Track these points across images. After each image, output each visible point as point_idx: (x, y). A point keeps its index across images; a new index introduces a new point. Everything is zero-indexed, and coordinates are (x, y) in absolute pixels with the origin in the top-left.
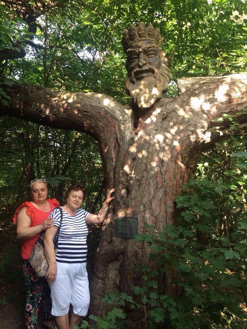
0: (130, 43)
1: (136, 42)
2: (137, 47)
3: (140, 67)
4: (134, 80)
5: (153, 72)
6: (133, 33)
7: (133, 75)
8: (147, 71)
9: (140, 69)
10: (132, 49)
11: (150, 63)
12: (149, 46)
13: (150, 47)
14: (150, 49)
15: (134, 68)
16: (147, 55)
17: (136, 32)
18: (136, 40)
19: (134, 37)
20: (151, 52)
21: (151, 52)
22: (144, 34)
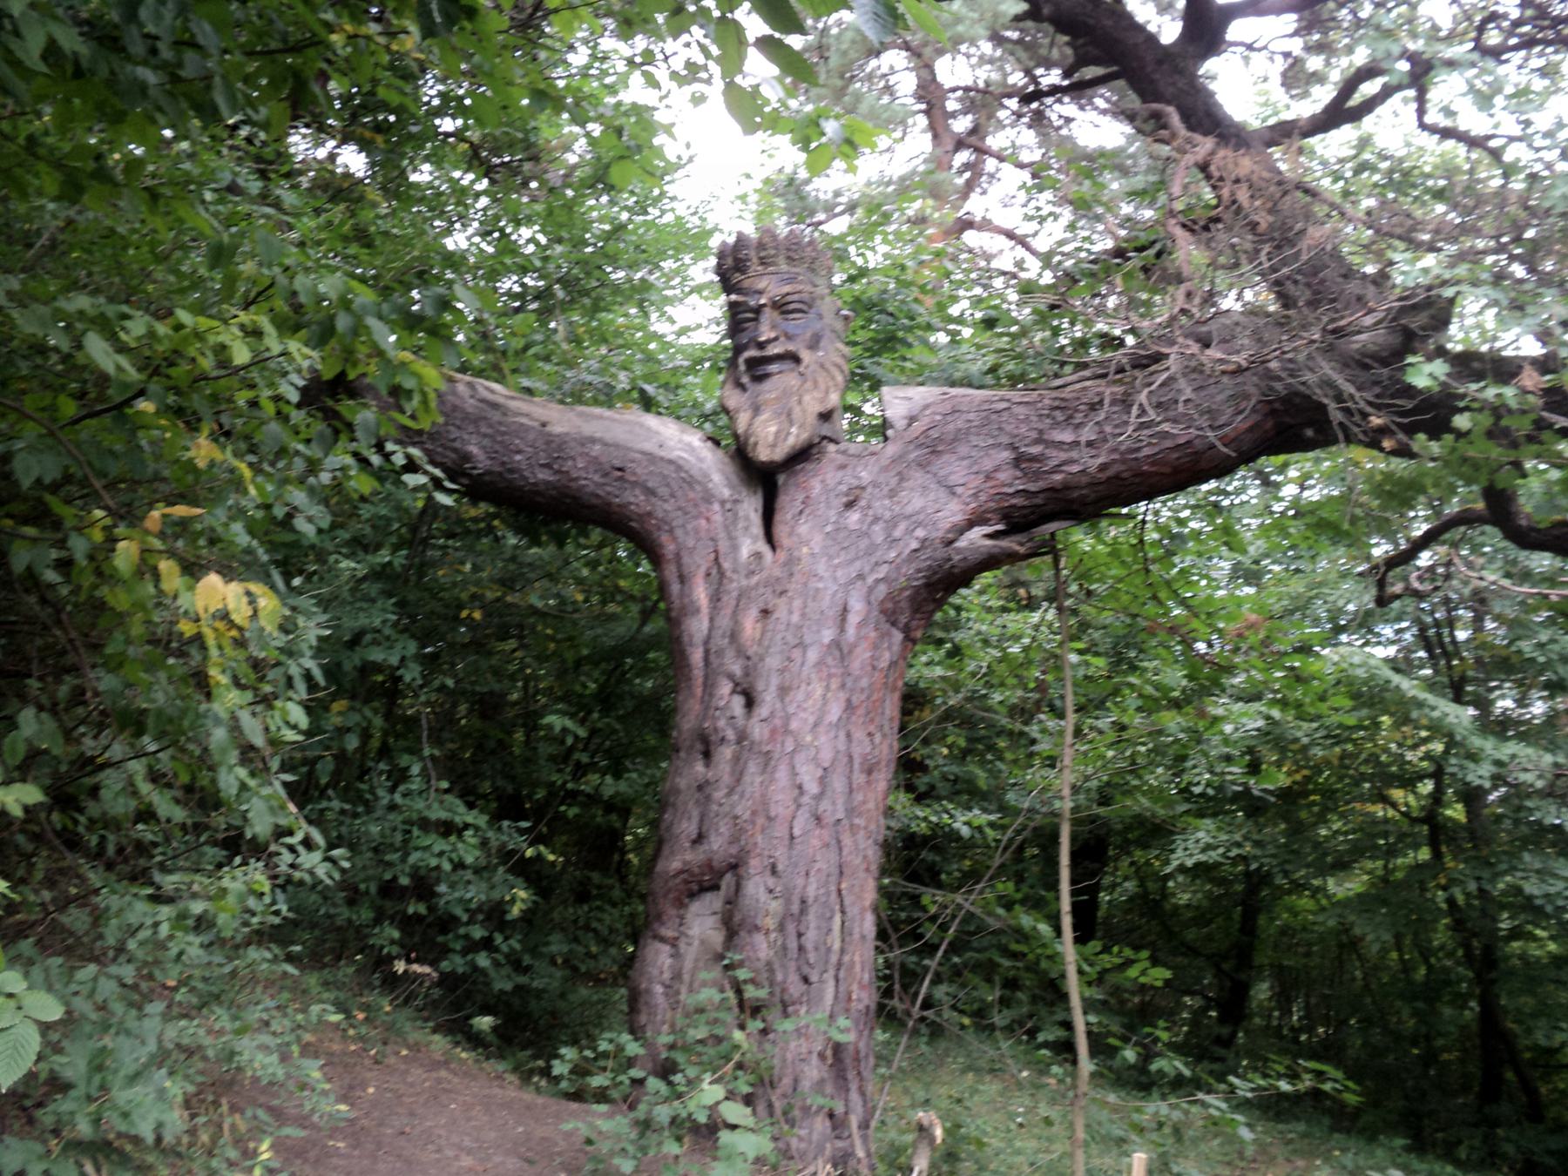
3: (761, 346)
4: (745, 380)
5: (796, 359)
7: (742, 367)
11: (789, 337)
12: (787, 289)
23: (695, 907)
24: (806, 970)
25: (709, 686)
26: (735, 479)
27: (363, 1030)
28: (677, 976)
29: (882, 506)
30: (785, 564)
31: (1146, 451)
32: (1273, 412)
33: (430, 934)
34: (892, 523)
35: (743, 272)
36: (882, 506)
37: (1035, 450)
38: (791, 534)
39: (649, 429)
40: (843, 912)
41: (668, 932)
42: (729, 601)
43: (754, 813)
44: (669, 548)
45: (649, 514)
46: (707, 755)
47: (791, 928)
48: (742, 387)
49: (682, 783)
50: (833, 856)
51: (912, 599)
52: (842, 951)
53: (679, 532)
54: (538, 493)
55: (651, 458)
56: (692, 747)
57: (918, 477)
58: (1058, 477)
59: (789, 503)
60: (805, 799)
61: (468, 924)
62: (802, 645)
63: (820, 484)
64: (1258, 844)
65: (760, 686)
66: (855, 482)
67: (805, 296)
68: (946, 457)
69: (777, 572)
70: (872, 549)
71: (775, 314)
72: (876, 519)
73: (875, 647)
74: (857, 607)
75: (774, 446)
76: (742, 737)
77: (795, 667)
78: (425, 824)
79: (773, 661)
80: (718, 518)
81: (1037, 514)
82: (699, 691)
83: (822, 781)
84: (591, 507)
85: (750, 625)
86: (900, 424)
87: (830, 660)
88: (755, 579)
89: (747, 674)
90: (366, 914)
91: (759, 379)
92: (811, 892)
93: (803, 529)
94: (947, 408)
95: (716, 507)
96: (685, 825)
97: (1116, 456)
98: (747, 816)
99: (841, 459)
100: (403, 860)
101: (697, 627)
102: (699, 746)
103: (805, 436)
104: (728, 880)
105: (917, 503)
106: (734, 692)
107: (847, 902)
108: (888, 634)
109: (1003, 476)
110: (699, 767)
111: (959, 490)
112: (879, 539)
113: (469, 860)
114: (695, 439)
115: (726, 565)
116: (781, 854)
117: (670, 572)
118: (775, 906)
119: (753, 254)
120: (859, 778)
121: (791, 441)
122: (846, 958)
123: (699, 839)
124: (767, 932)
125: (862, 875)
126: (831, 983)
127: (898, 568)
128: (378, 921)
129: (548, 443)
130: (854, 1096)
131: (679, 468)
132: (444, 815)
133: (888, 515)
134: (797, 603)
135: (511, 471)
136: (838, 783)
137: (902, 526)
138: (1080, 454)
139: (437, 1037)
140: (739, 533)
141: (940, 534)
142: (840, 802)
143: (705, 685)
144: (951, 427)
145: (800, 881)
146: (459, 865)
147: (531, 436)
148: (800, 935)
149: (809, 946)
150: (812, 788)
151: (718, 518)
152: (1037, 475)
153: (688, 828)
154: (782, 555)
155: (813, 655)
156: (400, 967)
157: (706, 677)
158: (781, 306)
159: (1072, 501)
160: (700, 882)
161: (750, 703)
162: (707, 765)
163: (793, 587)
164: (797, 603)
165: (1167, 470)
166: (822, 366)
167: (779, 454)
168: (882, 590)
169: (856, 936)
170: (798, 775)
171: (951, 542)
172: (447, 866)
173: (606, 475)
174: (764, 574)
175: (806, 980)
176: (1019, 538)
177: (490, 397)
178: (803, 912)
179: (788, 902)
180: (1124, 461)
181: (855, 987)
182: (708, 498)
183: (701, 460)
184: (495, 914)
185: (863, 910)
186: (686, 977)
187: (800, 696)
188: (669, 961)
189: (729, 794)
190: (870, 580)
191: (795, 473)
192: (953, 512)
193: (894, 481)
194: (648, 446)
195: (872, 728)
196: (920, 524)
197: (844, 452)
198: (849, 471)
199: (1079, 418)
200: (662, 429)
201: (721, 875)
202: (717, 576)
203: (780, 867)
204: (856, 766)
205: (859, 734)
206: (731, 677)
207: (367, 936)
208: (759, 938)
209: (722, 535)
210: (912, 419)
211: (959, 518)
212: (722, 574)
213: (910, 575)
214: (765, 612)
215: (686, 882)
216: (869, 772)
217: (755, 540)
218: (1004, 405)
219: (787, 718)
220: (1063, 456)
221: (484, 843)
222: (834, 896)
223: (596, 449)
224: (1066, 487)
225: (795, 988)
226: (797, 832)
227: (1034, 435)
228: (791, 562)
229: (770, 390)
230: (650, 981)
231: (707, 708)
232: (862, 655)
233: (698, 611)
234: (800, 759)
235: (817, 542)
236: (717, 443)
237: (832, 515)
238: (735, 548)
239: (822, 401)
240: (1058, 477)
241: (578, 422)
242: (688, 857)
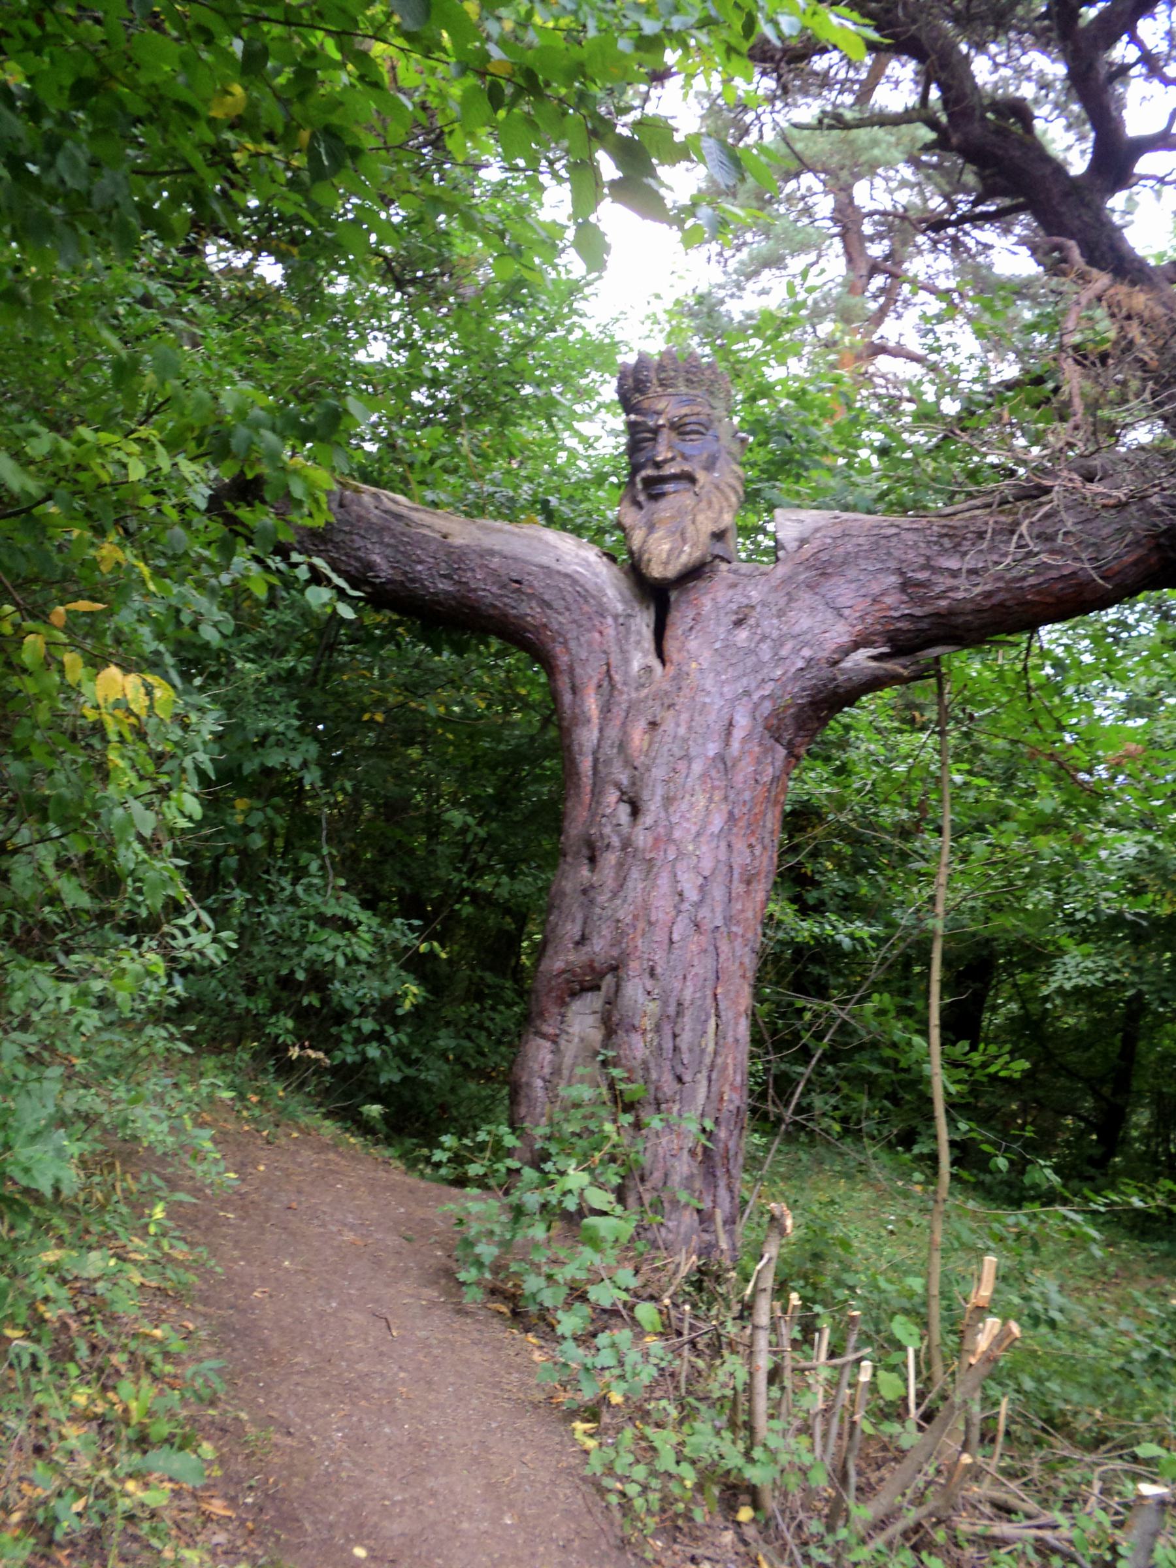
3: (658, 465)
4: (642, 498)
5: (690, 478)
7: (639, 486)
10: (639, 419)
11: (685, 458)
17: (653, 375)
23: (577, 1005)
24: (680, 1070)
25: (597, 793)
26: (628, 594)
27: (257, 1112)
28: (557, 1071)
29: (770, 625)
30: (674, 679)
31: (1032, 581)
32: (1159, 547)
33: (323, 1023)
34: (780, 642)
35: (642, 393)
36: (770, 625)
37: (922, 576)
38: (680, 650)
39: (547, 543)
40: (718, 1016)
41: (549, 1030)
42: (618, 712)
43: (636, 917)
44: (563, 660)
46: (592, 860)
47: (667, 1030)
48: (639, 505)
49: (568, 886)
50: (710, 962)
51: (796, 717)
52: (716, 1053)
53: (572, 644)
54: (439, 603)
55: (547, 570)
56: (578, 853)
57: (806, 598)
59: (680, 619)
60: (685, 906)
61: (360, 1016)
62: (687, 757)
63: (712, 600)
64: (1136, 970)
65: (646, 795)
66: (745, 601)
67: (703, 418)
68: (834, 580)
69: (666, 686)
70: (760, 665)
71: (673, 435)
72: (764, 638)
73: (759, 762)
74: (742, 721)
75: (666, 564)
76: (626, 844)
77: (679, 779)
78: (323, 921)
79: (659, 773)
80: (611, 632)
81: (922, 639)
82: (587, 798)
83: (702, 888)
84: (491, 617)
85: (638, 736)
86: (792, 546)
87: (713, 773)
89: (634, 784)
90: (260, 1004)
91: (655, 497)
92: (688, 995)
93: (693, 644)
94: (837, 532)
95: (610, 620)
96: (569, 926)
97: (1001, 584)
98: (628, 920)
100: (299, 954)
101: (587, 736)
102: (585, 852)
103: (697, 554)
104: (608, 981)
105: (805, 623)
106: (620, 800)
107: (722, 1006)
108: (772, 749)
109: (889, 600)
110: (585, 872)
111: (847, 612)
112: (766, 656)
113: (363, 955)
114: (591, 554)
115: (617, 678)
116: (659, 957)
117: (564, 682)
118: (653, 1007)
119: (653, 375)
120: (738, 887)
121: (684, 559)
122: (719, 1060)
123: (583, 940)
124: (644, 1032)
125: (738, 981)
126: (705, 1083)
127: (784, 686)
128: (274, 1011)
129: (449, 554)
130: (723, 1193)
131: (575, 582)
132: (339, 912)
133: (775, 634)
134: (684, 716)
135: (413, 581)
136: (718, 892)
137: (789, 645)
138: (964, 581)
139: (328, 1123)
140: (631, 647)
141: (826, 654)
142: (719, 910)
143: (593, 793)
144: (841, 550)
145: (677, 985)
146: (353, 960)
147: (433, 547)
148: (675, 1036)
149: (684, 1047)
150: (693, 895)
151: (611, 632)
152: (923, 601)
153: (572, 929)
154: (671, 670)
155: (697, 767)
156: (295, 1053)
157: (594, 784)
158: (679, 428)
159: (956, 627)
160: (581, 982)
161: (636, 811)
162: (592, 870)
164: (684, 716)
165: (1049, 600)
166: (717, 487)
167: (671, 572)
168: (767, 707)
169: (730, 1040)
170: (680, 884)
171: (836, 663)
172: (341, 962)
174: (654, 688)
175: (680, 1079)
176: (902, 660)
177: (394, 507)
178: (679, 1014)
179: (665, 1003)
180: (1008, 590)
181: (726, 1088)
183: (597, 575)
184: (386, 1009)
185: (737, 1016)
186: (566, 1073)
187: (684, 806)
188: (549, 1057)
189: (611, 899)
190: (756, 697)
191: (687, 590)
192: (840, 633)
193: (783, 602)
194: (545, 560)
195: (753, 840)
197: (735, 572)
198: (739, 589)
200: (559, 543)
201: (602, 975)
202: (609, 686)
203: (659, 970)
204: (736, 876)
205: (740, 845)
206: (618, 786)
207: (264, 1026)
208: (636, 1038)
209: (614, 648)
210: (803, 541)
211: (845, 639)
212: (613, 686)
213: (795, 693)
214: (653, 725)
215: (568, 981)
216: (748, 883)
217: (645, 656)
218: (894, 531)
219: (671, 827)
220: (950, 582)
221: (377, 940)
222: (709, 1000)
223: (495, 562)
224: (951, 612)
225: (669, 1086)
226: (676, 937)
227: (922, 561)
228: (680, 677)
229: (665, 509)
230: (531, 1075)
231: (593, 816)
232: (746, 768)
234: (681, 867)
236: (613, 559)
237: (722, 632)
238: (627, 661)
239: (716, 521)
240: (943, 603)
241: (478, 534)
242: (571, 958)
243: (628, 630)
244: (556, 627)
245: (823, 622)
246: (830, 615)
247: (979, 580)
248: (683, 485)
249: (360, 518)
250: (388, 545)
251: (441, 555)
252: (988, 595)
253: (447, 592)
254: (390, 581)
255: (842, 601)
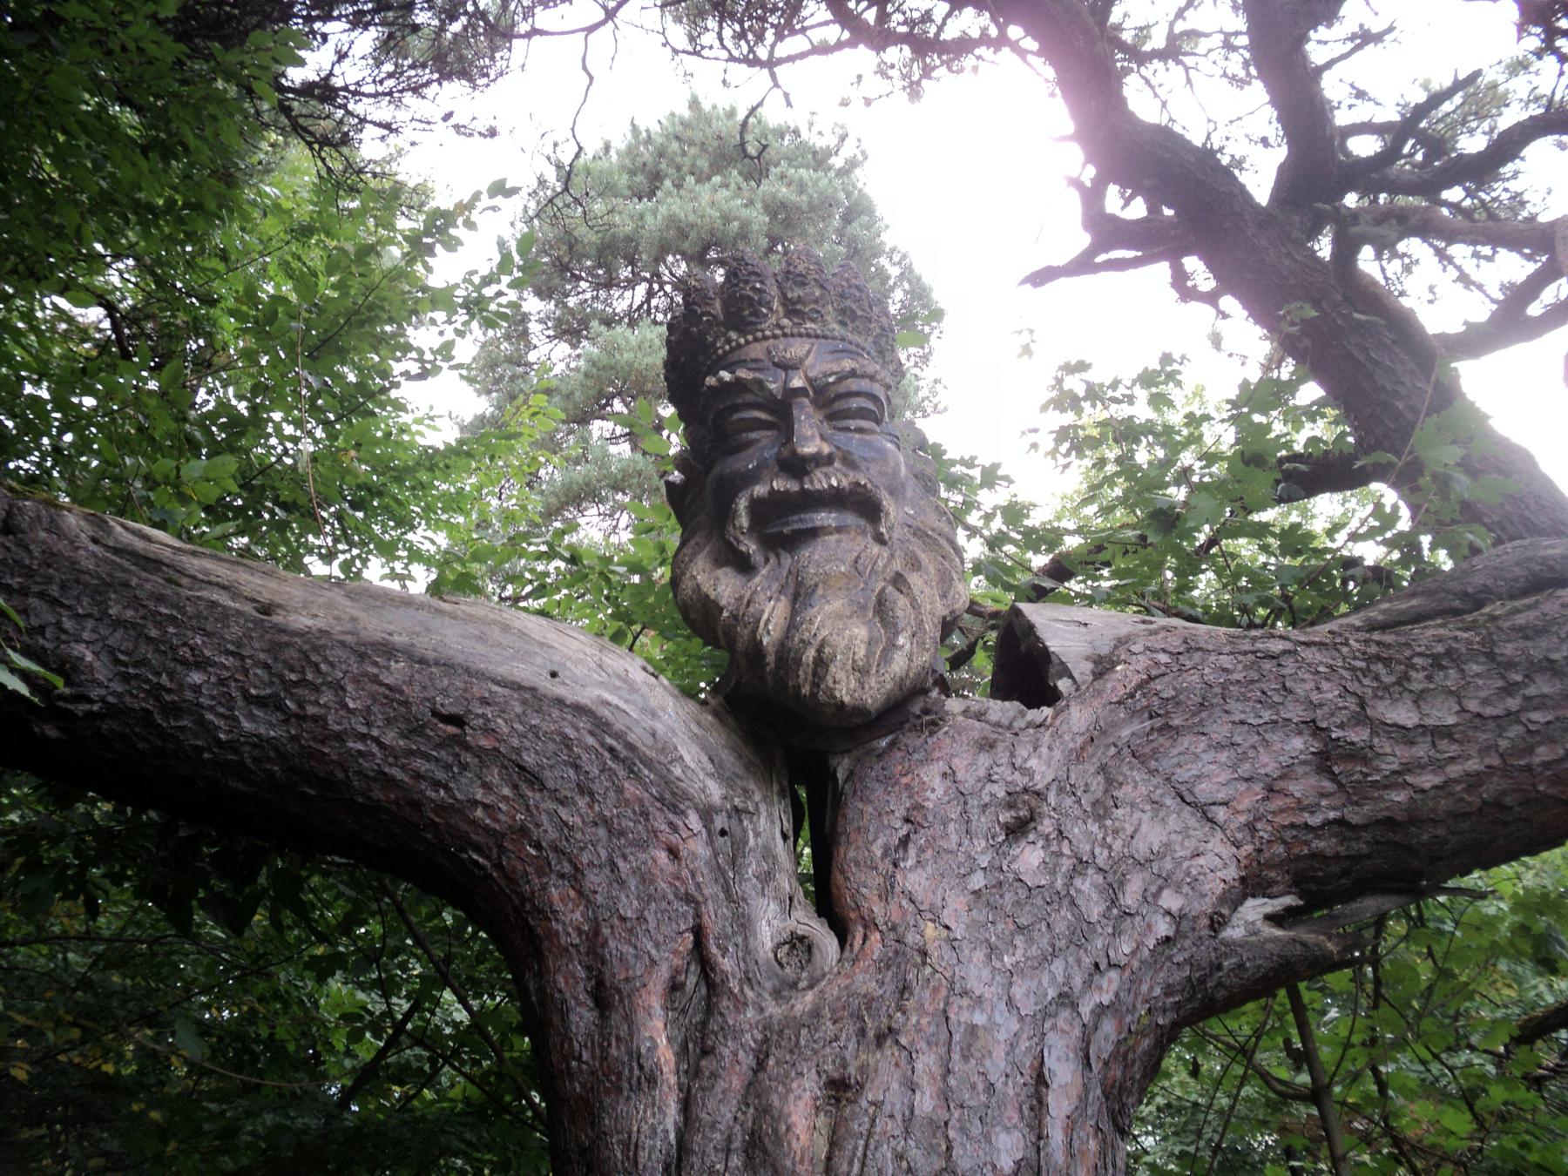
0: (729, 341)
1: (765, 338)
2: (776, 365)
4: (750, 546)
6: (754, 289)
7: (744, 521)
8: (836, 499)
9: (793, 486)
10: (743, 373)
11: (850, 463)
12: (848, 364)
13: (853, 373)
14: (853, 385)
15: (750, 479)
16: (831, 417)
17: (774, 291)
18: (767, 326)
19: (756, 314)
20: (855, 403)
21: (855, 403)
22: (816, 301)
26: (727, 757)
30: (885, 964)
31: (1543, 754)
35: (742, 326)
36: (1083, 834)
37: (1358, 736)
38: (886, 894)
39: (523, 635)
42: (734, 1061)
44: (570, 917)
45: (523, 831)
55: (530, 695)
58: (1399, 797)
66: (1021, 780)
68: (1185, 742)
69: (865, 981)
70: (1081, 933)
72: (1081, 865)
74: (1063, 1072)
75: (862, 671)
80: (698, 848)
86: (1082, 670)
88: (805, 1002)
93: (915, 880)
95: (694, 821)
97: (1496, 762)
99: (977, 729)
105: (1151, 836)
109: (1296, 789)
111: (1221, 814)
115: (727, 964)
117: (570, 981)
121: (899, 664)
127: (1135, 981)
129: (275, 649)
131: (601, 726)
134: (927, 1062)
135: (174, 710)
140: (750, 887)
147: (235, 631)
151: (698, 848)
163: (916, 1021)
164: (927, 1062)
167: (873, 693)
173: (415, 729)
177: (139, 545)
180: (1506, 770)
182: (673, 799)
190: (1086, 1009)
194: (524, 672)
196: (1166, 881)
199: (1418, 681)
202: (704, 985)
214: (840, 1089)
218: (1289, 646)
220: (1404, 753)
223: (397, 672)
224: (1414, 819)
228: (904, 961)
233: (652, 1080)
235: (956, 909)
238: (744, 923)
240: (1399, 797)
243: (739, 847)
244: (551, 833)
245: (1185, 832)
246: (1190, 817)
247: (1453, 749)
248: (850, 519)
249: (50, 557)
250: (118, 623)
251: (256, 649)
252: (1474, 781)
253: (260, 742)
254: (112, 711)
255: (1205, 791)
